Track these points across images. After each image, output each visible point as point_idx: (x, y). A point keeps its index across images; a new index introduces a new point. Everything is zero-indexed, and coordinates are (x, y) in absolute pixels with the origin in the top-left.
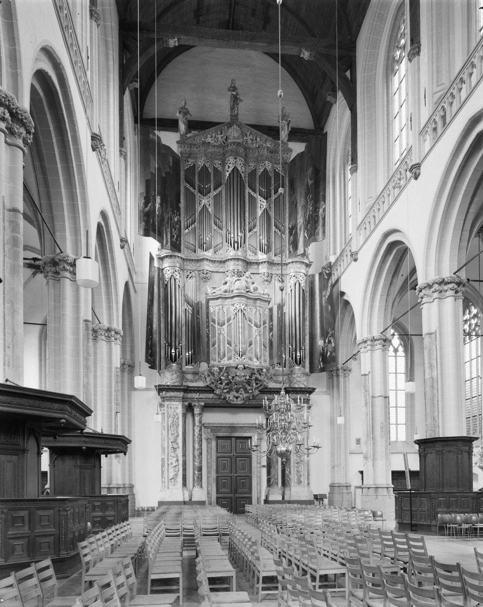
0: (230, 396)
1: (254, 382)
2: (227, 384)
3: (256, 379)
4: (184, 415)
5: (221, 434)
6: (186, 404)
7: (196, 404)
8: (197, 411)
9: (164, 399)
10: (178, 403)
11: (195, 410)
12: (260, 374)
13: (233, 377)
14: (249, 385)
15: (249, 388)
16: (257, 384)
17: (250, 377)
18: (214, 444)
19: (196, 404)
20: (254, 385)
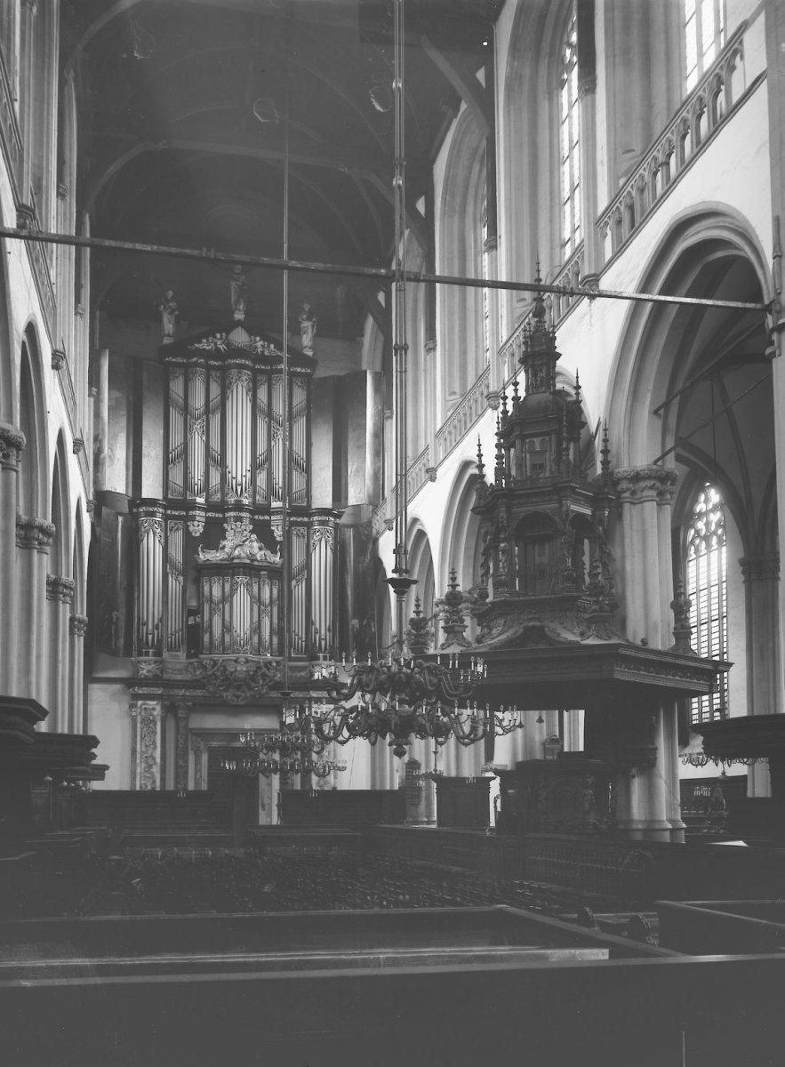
0: (228, 695)
1: (260, 677)
2: (223, 681)
3: (264, 675)
4: (164, 720)
5: (215, 744)
6: (167, 703)
7: (182, 704)
8: (181, 714)
9: (136, 697)
10: (155, 702)
11: (180, 712)
12: (268, 669)
13: (232, 672)
14: (254, 681)
15: (253, 685)
16: (264, 680)
17: (255, 672)
18: (205, 757)
19: (182, 704)
20: (261, 682)
